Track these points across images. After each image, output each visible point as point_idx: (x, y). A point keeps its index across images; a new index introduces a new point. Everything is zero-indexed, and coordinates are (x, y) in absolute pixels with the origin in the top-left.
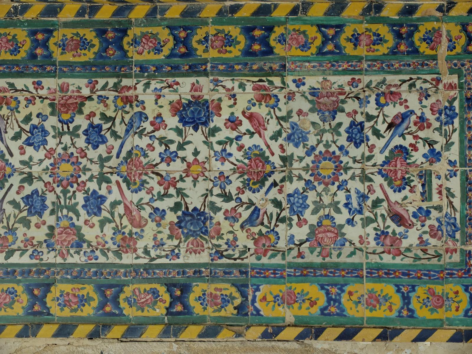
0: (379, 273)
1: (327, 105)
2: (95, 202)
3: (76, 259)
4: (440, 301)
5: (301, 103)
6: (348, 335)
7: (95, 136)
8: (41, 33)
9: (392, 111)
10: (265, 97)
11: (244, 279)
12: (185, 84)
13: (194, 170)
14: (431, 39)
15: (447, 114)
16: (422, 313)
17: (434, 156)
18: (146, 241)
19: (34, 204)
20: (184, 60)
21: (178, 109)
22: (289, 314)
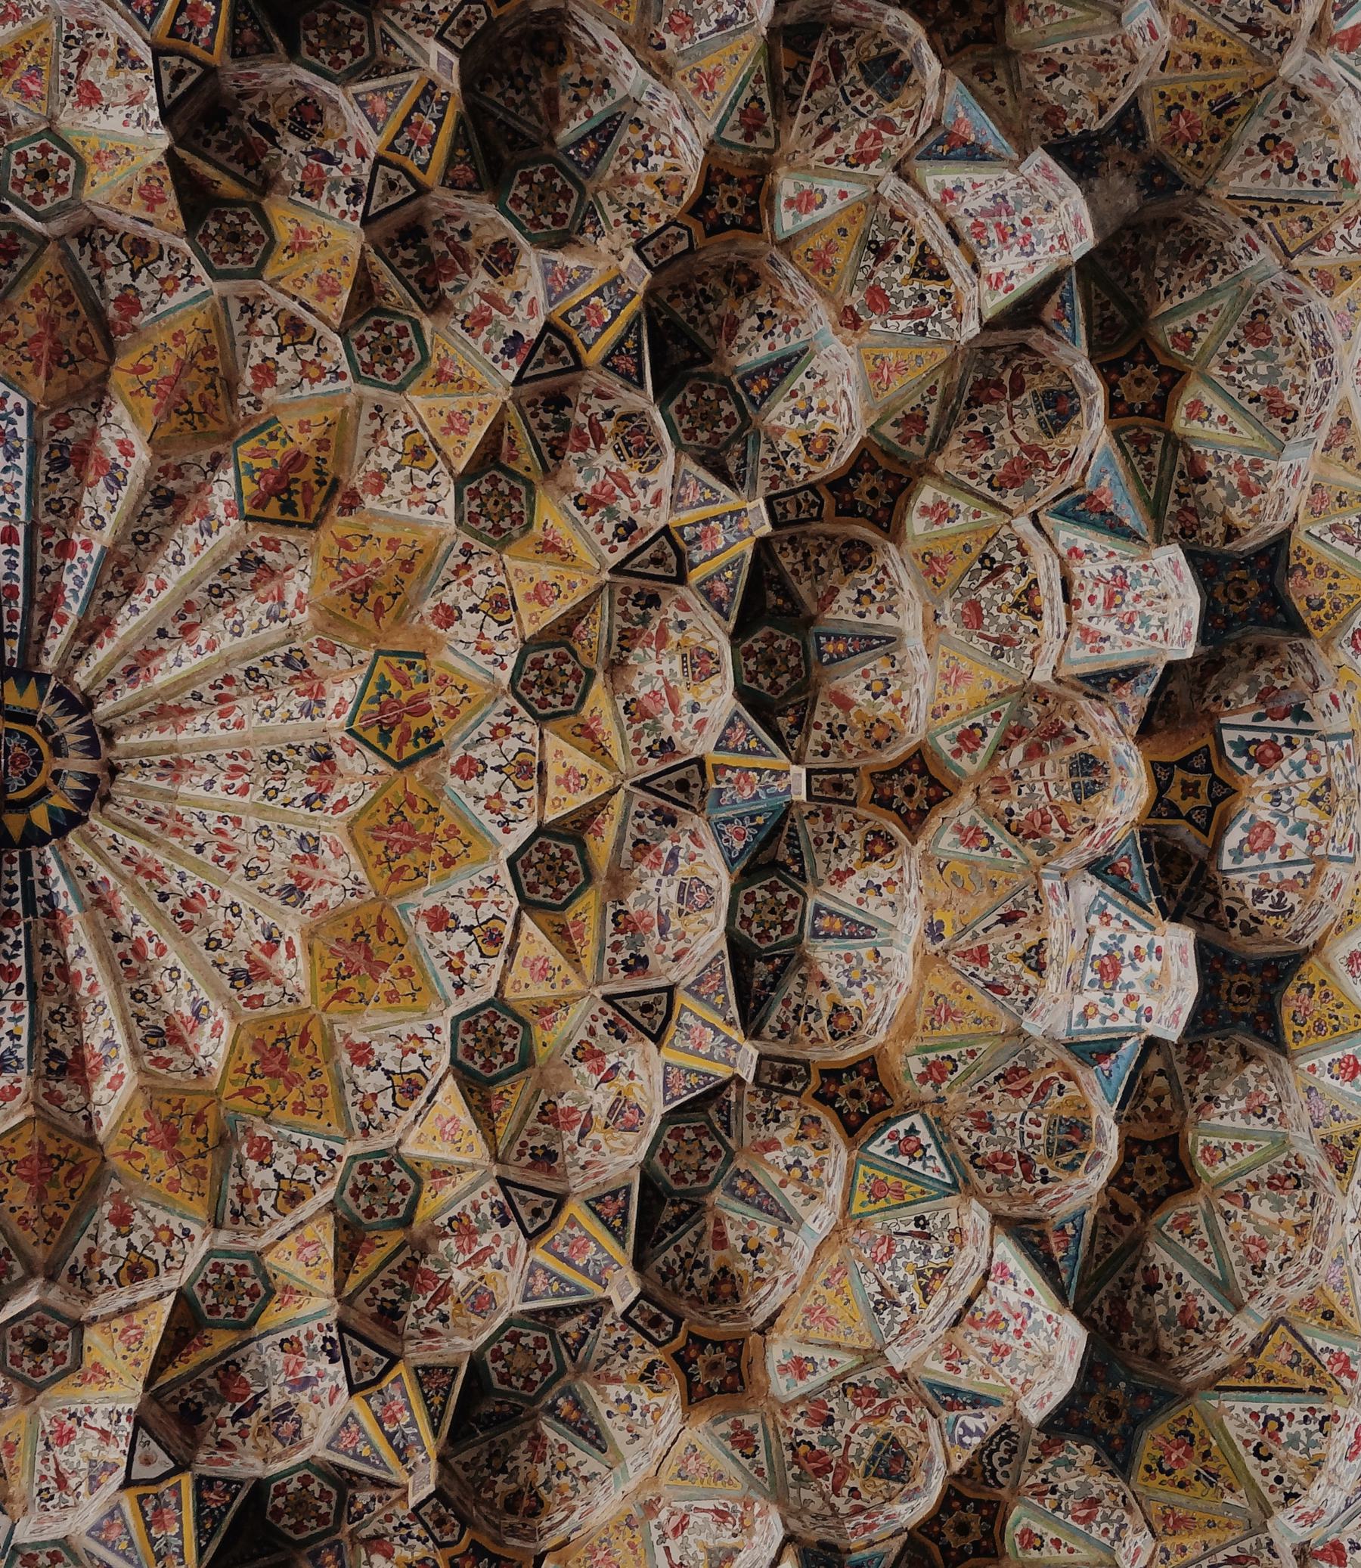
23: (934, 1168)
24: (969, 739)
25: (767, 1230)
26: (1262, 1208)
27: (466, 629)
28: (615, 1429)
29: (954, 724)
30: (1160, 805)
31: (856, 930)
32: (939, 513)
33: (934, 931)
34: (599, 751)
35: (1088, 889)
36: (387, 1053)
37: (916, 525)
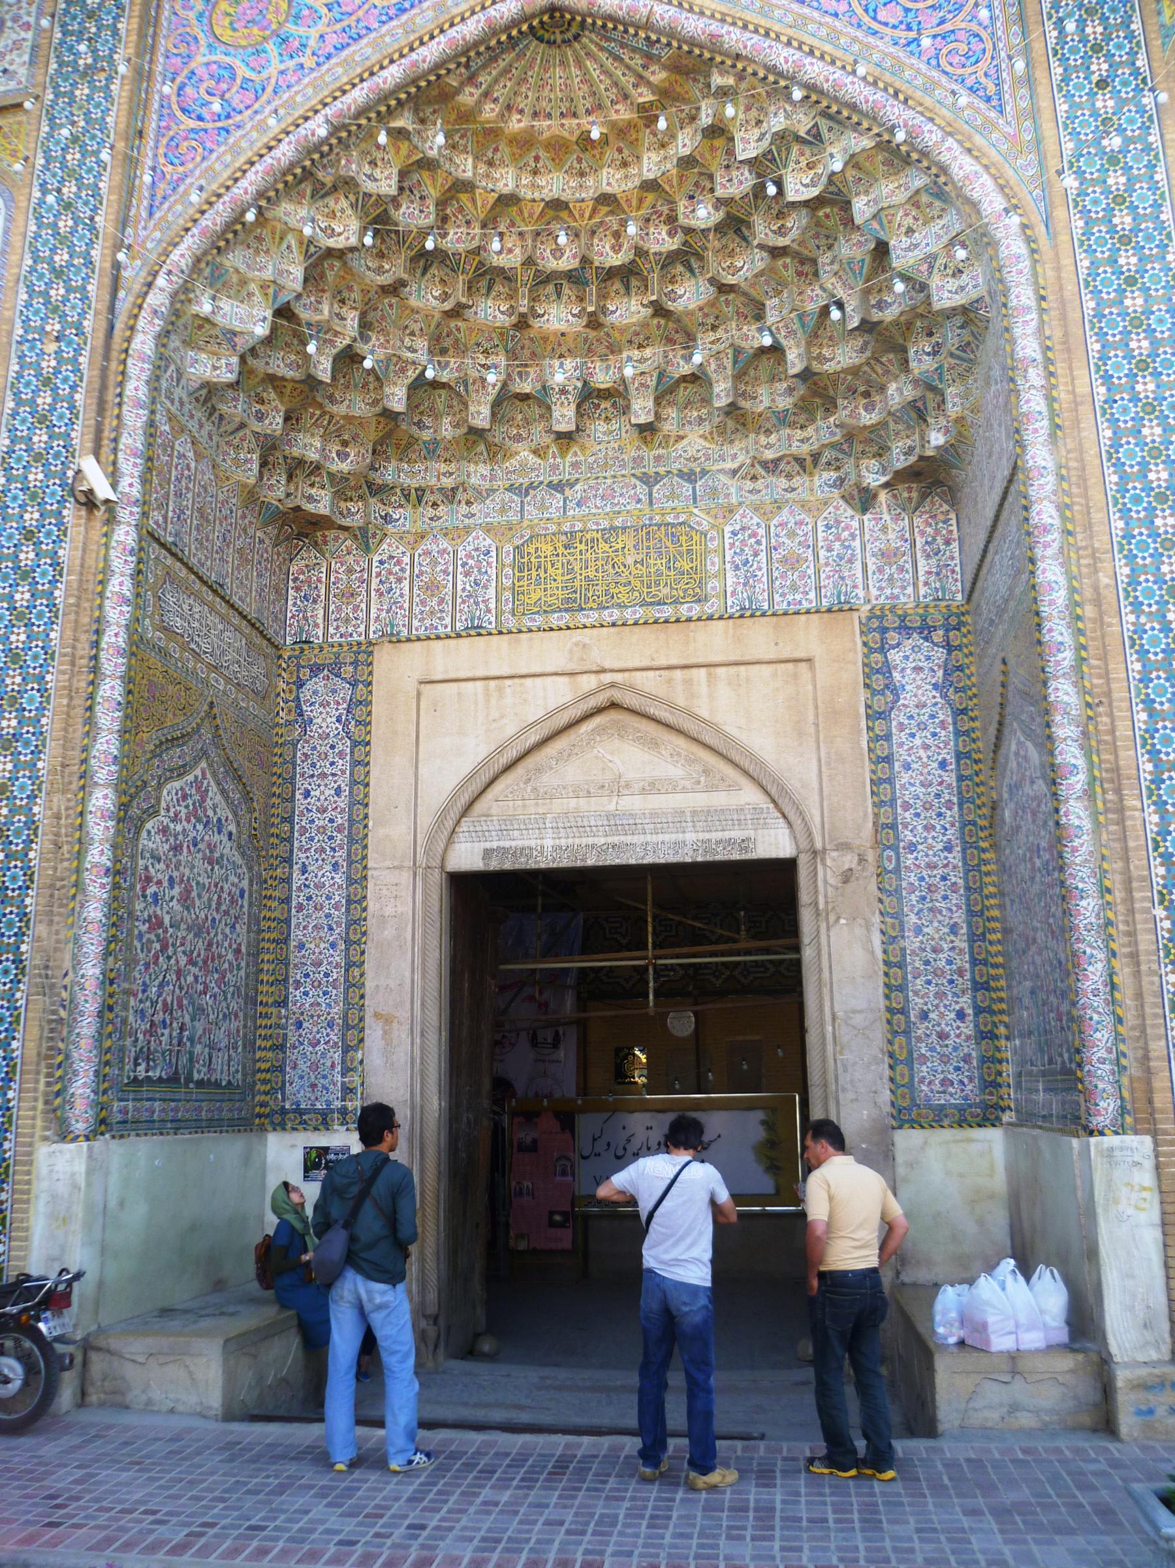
0: (912, 1078)
1: (967, 1059)
2: (929, 982)
3: (910, 977)
4: (903, 1097)
5: (966, 1050)
6: (891, 1067)
7: (951, 982)
8: (985, 963)
9: (966, 1081)
10: (968, 1038)
11: (907, 1033)
12: (970, 1011)
13: (942, 1015)
14: (991, 1094)
15: (966, 1098)
16: (899, 1091)
17: (951, 1095)
18: (917, 1000)
19: (927, 963)
20: (978, 1011)
21: (962, 1009)
22: (896, 1047)
23: (510, 345)
24: (608, 335)
25: (484, 291)
26: (520, 417)
27: (616, 155)
28: (428, 276)
29: (611, 332)
30: (599, 390)
31: (559, 295)
32: (659, 326)
33: (563, 334)
34: (590, 218)
35: (579, 384)
36: (499, 155)
37: (655, 321)
